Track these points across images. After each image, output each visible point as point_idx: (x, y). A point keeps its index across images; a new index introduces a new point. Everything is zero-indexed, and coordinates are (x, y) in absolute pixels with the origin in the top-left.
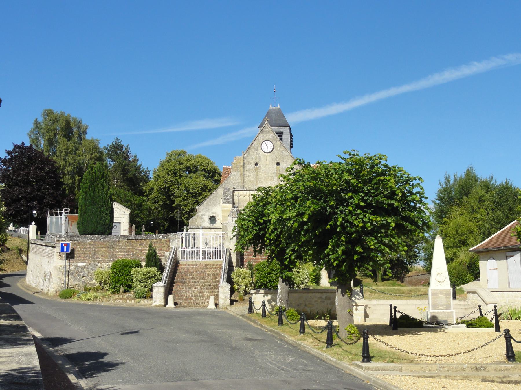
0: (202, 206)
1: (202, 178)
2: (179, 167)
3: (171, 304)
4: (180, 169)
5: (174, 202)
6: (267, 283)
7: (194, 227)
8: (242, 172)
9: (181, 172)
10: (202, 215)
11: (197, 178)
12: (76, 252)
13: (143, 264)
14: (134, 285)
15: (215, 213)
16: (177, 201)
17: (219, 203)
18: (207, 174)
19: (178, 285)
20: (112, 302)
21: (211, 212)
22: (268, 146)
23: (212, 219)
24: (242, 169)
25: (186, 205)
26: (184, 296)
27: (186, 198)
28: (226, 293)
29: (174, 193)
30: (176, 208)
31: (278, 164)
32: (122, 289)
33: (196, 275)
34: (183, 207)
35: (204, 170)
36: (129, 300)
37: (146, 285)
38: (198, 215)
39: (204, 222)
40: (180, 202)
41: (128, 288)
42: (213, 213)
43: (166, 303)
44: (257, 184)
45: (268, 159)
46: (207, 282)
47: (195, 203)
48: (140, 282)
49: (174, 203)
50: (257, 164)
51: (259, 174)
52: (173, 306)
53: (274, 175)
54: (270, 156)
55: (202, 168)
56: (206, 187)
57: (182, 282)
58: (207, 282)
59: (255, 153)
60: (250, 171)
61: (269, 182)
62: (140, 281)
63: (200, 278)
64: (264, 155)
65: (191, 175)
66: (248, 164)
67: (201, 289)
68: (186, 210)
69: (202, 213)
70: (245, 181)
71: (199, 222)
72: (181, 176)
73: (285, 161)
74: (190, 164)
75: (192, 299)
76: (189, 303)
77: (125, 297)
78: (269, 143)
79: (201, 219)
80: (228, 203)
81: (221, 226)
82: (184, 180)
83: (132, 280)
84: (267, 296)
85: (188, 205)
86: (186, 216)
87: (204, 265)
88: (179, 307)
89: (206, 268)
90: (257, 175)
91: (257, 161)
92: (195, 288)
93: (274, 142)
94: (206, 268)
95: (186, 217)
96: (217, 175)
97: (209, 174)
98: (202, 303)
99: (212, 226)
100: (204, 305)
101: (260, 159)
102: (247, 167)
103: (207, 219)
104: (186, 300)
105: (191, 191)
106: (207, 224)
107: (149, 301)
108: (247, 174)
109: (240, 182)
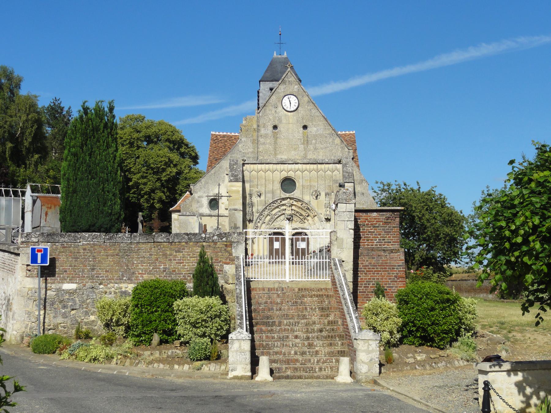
0: (198, 185)
1: (166, 150)
2: (136, 135)
3: (263, 374)
4: (138, 139)
5: (130, 180)
6: (429, 325)
7: (188, 213)
8: (255, 138)
9: (140, 143)
10: (199, 197)
11: (159, 150)
12: (58, 264)
13: (190, 286)
14: (180, 330)
16: (135, 178)
17: (223, 181)
18: (171, 145)
19: (261, 331)
20: (142, 366)
22: (291, 102)
23: (214, 203)
24: (255, 134)
25: (145, 184)
26: (280, 353)
27: (145, 175)
28: (373, 351)
29: (130, 168)
30: (133, 187)
31: (305, 127)
32: (156, 338)
33: (289, 309)
34: (142, 186)
35: (168, 140)
36: (179, 364)
37: (205, 333)
39: (202, 206)
40: (138, 179)
41: (168, 336)
43: (254, 371)
44: (276, 154)
45: (291, 121)
46: (314, 323)
47: (157, 181)
48: (195, 327)
49: (131, 181)
50: (275, 127)
51: (279, 141)
52: (270, 379)
54: (293, 116)
55: (166, 137)
56: (171, 161)
57: (267, 324)
58: (314, 323)
59: (273, 112)
60: (266, 136)
61: (293, 152)
62: (194, 325)
63: (298, 315)
64: (286, 115)
65: (151, 146)
66: (264, 127)
67: (308, 338)
68: (145, 190)
69: (199, 194)
70: (260, 150)
71: (194, 207)
72: (139, 147)
73: (314, 123)
74: (150, 132)
75: (297, 360)
76: (296, 369)
77: (165, 356)
78: (293, 99)
79: (198, 202)
80: (237, 181)
81: (226, 213)
82: (142, 153)
83: (175, 320)
84: (516, 374)
85: (149, 183)
86: (146, 197)
87: (297, 290)
88: (279, 378)
89: (303, 296)
90: (275, 143)
91: (276, 123)
92: (296, 337)
93: (299, 97)
94: (303, 296)
95: (146, 199)
96: (184, 147)
97: (174, 145)
98: (321, 369)
100: (323, 373)
101: (280, 120)
102: (263, 131)
103: (205, 202)
104: (288, 362)
105: (152, 166)
106: (205, 209)
107: (218, 367)
108: (262, 140)
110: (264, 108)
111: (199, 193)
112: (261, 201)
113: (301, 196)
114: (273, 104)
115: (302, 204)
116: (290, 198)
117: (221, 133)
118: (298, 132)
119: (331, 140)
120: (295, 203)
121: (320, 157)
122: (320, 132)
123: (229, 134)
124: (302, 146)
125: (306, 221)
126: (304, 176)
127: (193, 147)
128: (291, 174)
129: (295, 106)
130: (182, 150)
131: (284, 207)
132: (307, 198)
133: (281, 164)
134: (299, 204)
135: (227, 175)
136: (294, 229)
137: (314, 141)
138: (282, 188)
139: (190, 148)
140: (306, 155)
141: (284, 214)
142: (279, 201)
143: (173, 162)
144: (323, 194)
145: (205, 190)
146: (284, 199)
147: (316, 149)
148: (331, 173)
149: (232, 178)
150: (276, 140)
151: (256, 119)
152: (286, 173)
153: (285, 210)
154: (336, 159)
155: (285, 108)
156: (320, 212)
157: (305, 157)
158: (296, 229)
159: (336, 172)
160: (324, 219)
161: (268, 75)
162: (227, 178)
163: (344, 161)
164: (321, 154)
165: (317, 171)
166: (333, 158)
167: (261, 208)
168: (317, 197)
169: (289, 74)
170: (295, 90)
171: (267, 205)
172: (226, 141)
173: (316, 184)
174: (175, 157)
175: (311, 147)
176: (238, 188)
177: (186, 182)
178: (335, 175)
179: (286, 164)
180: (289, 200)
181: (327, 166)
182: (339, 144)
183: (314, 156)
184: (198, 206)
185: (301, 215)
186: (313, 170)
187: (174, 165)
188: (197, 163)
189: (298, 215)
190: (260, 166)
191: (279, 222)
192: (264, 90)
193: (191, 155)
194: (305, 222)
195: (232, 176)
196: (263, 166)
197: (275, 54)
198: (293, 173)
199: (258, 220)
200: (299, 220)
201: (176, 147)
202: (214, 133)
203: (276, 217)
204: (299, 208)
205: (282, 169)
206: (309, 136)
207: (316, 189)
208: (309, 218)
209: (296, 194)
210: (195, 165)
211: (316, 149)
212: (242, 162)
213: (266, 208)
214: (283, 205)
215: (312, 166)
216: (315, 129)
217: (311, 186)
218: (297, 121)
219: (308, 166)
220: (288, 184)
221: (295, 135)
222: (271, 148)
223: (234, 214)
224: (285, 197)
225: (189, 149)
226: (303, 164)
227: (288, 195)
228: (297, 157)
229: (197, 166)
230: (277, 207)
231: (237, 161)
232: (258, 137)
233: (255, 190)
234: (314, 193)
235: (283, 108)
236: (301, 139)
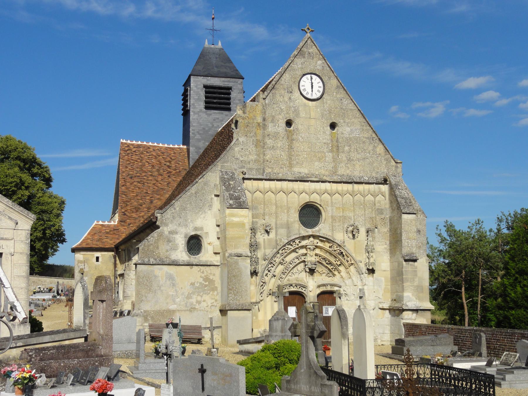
1: (17, 169)
7: (152, 261)
8: (259, 137)
10: (171, 232)
15: (201, 229)
17: (211, 206)
21: (191, 226)
22: (311, 86)
23: (194, 244)
24: (260, 132)
31: (333, 126)
35: (18, 158)
38: (161, 235)
39: (175, 248)
42: (196, 229)
44: (291, 166)
45: (313, 115)
50: (289, 123)
51: (296, 144)
55: (15, 154)
56: (22, 183)
59: (286, 99)
60: (276, 136)
61: (316, 163)
64: (305, 105)
66: (272, 121)
69: (171, 227)
70: (268, 157)
71: (163, 250)
73: (347, 120)
79: (169, 241)
81: (216, 260)
90: (291, 147)
91: (291, 116)
93: (325, 79)
96: (37, 166)
99: (194, 259)
101: (297, 112)
102: (271, 128)
103: (181, 242)
106: (181, 254)
108: (269, 142)
109: (256, 161)
110: (273, 91)
111: (170, 225)
112: (270, 241)
113: (330, 234)
114: (285, 86)
115: (330, 247)
116: (314, 237)
117: (134, 142)
118: (324, 132)
119: (371, 148)
120: (320, 244)
121: (357, 173)
122: (356, 134)
123: (145, 143)
124: (330, 154)
125: (336, 273)
126: (334, 201)
127: (46, 167)
128: (315, 198)
129: (319, 91)
130: (35, 170)
131: (304, 251)
132: (339, 237)
133: (301, 181)
134: (327, 246)
135: (217, 196)
136: (319, 286)
137: (347, 148)
138: (300, 221)
139: (43, 168)
140: (335, 168)
141: (304, 261)
142: (297, 241)
143: (24, 183)
144: (363, 231)
145: (180, 220)
146: (304, 238)
147: (350, 160)
148: (372, 198)
149: (231, 202)
150: (292, 143)
151: (260, 107)
152: (307, 197)
153: (306, 254)
154: (380, 177)
155: (304, 93)
156: (358, 258)
157: (335, 173)
158: (324, 285)
159: (380, 198)
160: (364, 270)
161: (200, 68)
162: (216, 203)
163: (393, 180)
164: (358, 167)
165: (353, 194)
166: (374, 175)
167: (269, 252)
168: (354, 236)
169: (309, 41)
170: (318, 67)
171: (279, 247)
172: (142, 153)
173: (351, 215)
174: (26, 177)
175: (343, 156)
176: (242, 219)
177: (40, 207)
178: (379, 202)
179: (307, 181)
180: (311, 239)
181: (367, 187)
182: (383, 154)
183: (348, 171)
184: (168, 248)
185: (330, 263)
186: (348, 192)
187: (26, 187)
188: (50, 186)
189: (324, 263)
190: (267, 184)
191: (296, 276)
192: (196, 87)
193: (44, 176)
194: (334, 275)
195: (231, 199)
196: (272, 184)
197: (206, 43)
198: (317, 197)
199: (266, 272)
200: (325, 270)
201: (27, 166)
202: (124, 141)
203: (292, 266)
204: (327, 251)
205: (301, 190)
206: (340, 140)
207: (352, 222)
208: (341, 268)
209: (323, 228)
210: (48, 188)
211: (350, 160)
212: (242, 176)
213: (278, 252)
214: (302, 247)
215: (346, 187)
216: (348, 129)
217: (345, 218)
218: (322, 116)
219: (340, 187)
220: (310, 213)
221: (319, 136)
222: (284, 156)
223: (237, 263)
224: (307, 234)
225: (42, 170)
226: (333, 182)
227: (310, 232)
228: (323, 172)
229: (51, 190)
230: (294, 251)
231: (234, 174)
232: (264, 137)
233: (260, 222)
234: (351, 229)
235: (301, 94)
236: (328, 144)
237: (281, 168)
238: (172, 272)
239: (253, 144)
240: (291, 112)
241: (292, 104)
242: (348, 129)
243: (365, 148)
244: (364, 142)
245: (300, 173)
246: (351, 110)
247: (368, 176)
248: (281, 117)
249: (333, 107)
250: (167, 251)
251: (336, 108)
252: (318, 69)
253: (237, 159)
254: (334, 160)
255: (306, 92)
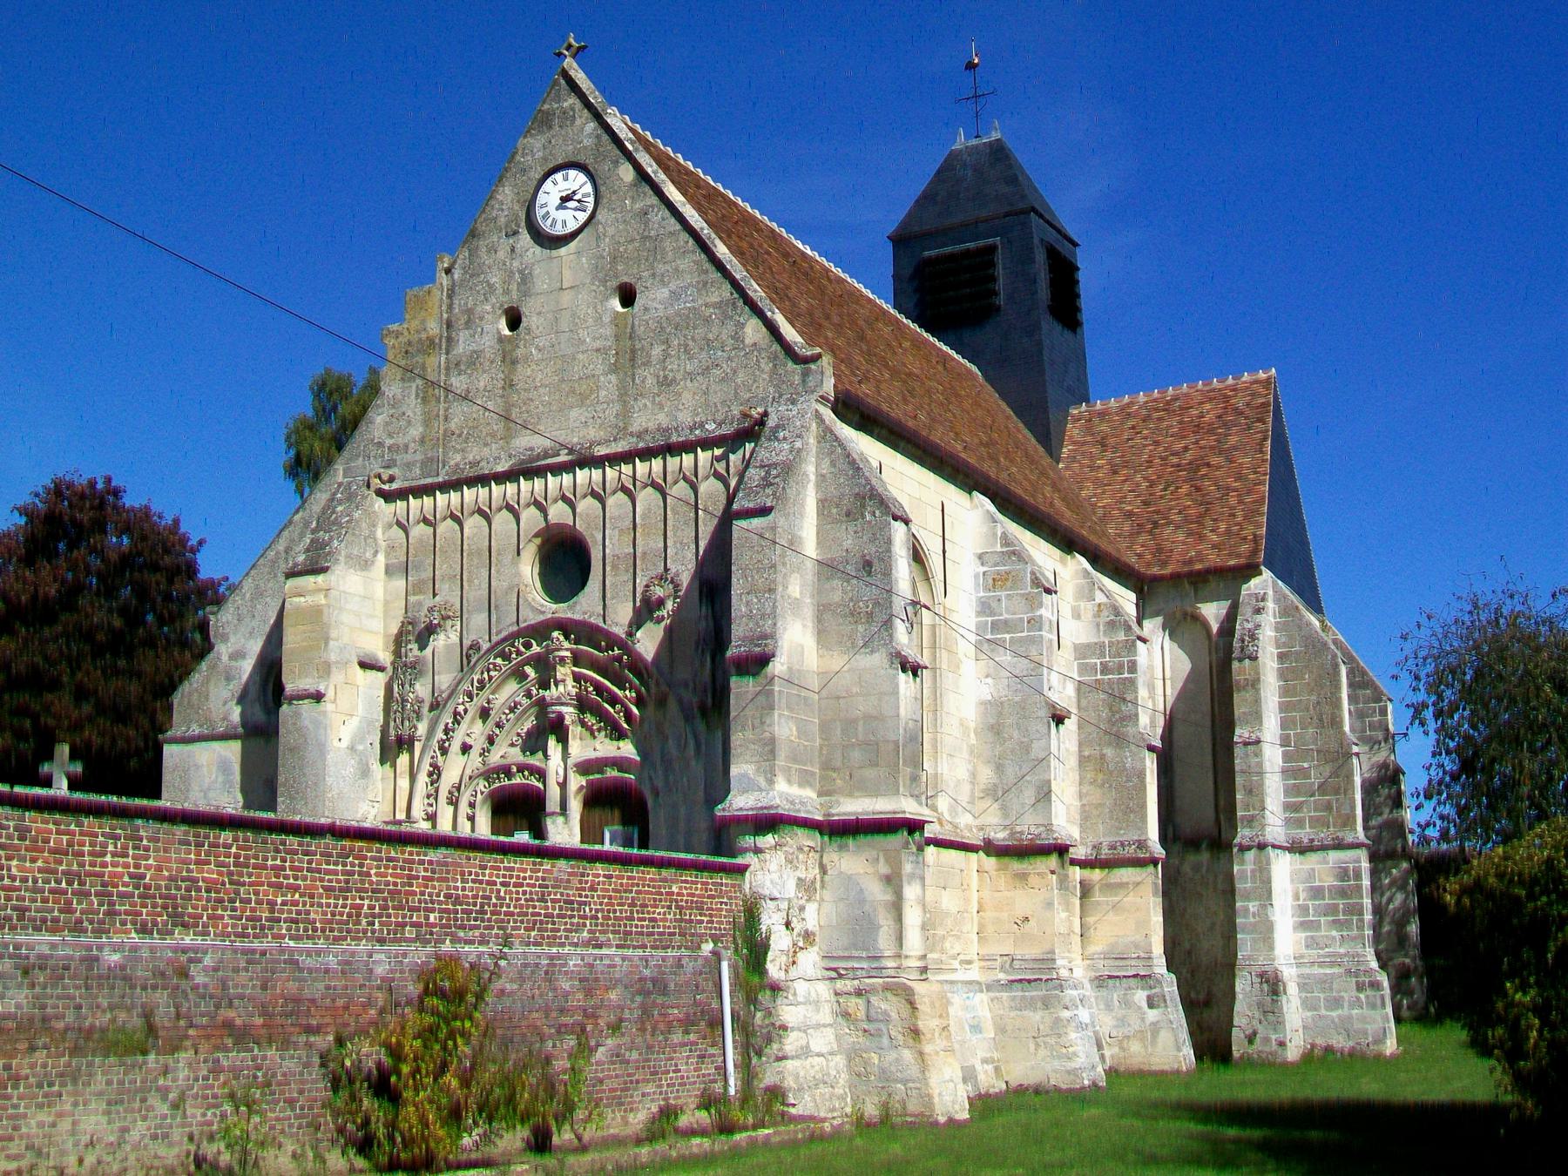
50: (514, 321)
51: (522, 372)
53: (600, 369)
60: (474, 360)
73: (660, 268)
90: (509, 385)
93: (603, 168)
102: (464, 344)
111: (232, 639)
119: (727, 331)
124: (613, 378)
140: (625, 414)
147: (665, 383)
150: (513, 371)
164: (686, 396)
183: (662, 419)
206: (640, 331)
216: (664, 293)
221: (583, 334)
228: (592, 433)
237: (486, 445)
238: (229, 755)
239: (417, 396)
240: (514, 287)
241: (516, 264)
242: (664, 293)
243: (710, 336)
244: (707, 320)
245: (532, 449)
246: (672, 234)
247: (719, 417)
248: (488, 308)
249: (622, 240)
250: (225, 703)
251: (632, 240)
252: (585, 148)
253: (380, 444)
254: (623, 395)
255: (549, 222)
